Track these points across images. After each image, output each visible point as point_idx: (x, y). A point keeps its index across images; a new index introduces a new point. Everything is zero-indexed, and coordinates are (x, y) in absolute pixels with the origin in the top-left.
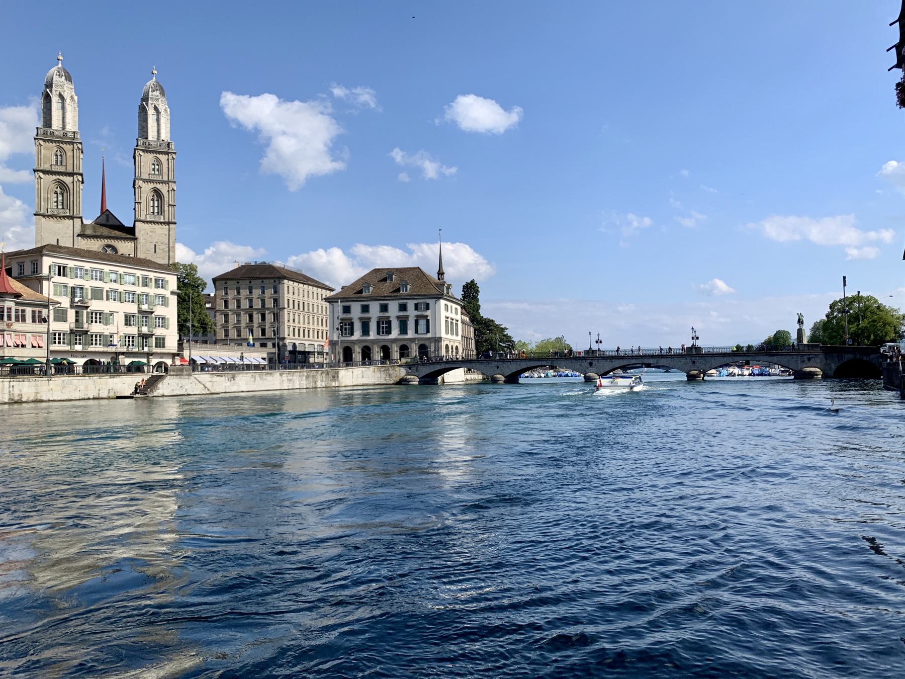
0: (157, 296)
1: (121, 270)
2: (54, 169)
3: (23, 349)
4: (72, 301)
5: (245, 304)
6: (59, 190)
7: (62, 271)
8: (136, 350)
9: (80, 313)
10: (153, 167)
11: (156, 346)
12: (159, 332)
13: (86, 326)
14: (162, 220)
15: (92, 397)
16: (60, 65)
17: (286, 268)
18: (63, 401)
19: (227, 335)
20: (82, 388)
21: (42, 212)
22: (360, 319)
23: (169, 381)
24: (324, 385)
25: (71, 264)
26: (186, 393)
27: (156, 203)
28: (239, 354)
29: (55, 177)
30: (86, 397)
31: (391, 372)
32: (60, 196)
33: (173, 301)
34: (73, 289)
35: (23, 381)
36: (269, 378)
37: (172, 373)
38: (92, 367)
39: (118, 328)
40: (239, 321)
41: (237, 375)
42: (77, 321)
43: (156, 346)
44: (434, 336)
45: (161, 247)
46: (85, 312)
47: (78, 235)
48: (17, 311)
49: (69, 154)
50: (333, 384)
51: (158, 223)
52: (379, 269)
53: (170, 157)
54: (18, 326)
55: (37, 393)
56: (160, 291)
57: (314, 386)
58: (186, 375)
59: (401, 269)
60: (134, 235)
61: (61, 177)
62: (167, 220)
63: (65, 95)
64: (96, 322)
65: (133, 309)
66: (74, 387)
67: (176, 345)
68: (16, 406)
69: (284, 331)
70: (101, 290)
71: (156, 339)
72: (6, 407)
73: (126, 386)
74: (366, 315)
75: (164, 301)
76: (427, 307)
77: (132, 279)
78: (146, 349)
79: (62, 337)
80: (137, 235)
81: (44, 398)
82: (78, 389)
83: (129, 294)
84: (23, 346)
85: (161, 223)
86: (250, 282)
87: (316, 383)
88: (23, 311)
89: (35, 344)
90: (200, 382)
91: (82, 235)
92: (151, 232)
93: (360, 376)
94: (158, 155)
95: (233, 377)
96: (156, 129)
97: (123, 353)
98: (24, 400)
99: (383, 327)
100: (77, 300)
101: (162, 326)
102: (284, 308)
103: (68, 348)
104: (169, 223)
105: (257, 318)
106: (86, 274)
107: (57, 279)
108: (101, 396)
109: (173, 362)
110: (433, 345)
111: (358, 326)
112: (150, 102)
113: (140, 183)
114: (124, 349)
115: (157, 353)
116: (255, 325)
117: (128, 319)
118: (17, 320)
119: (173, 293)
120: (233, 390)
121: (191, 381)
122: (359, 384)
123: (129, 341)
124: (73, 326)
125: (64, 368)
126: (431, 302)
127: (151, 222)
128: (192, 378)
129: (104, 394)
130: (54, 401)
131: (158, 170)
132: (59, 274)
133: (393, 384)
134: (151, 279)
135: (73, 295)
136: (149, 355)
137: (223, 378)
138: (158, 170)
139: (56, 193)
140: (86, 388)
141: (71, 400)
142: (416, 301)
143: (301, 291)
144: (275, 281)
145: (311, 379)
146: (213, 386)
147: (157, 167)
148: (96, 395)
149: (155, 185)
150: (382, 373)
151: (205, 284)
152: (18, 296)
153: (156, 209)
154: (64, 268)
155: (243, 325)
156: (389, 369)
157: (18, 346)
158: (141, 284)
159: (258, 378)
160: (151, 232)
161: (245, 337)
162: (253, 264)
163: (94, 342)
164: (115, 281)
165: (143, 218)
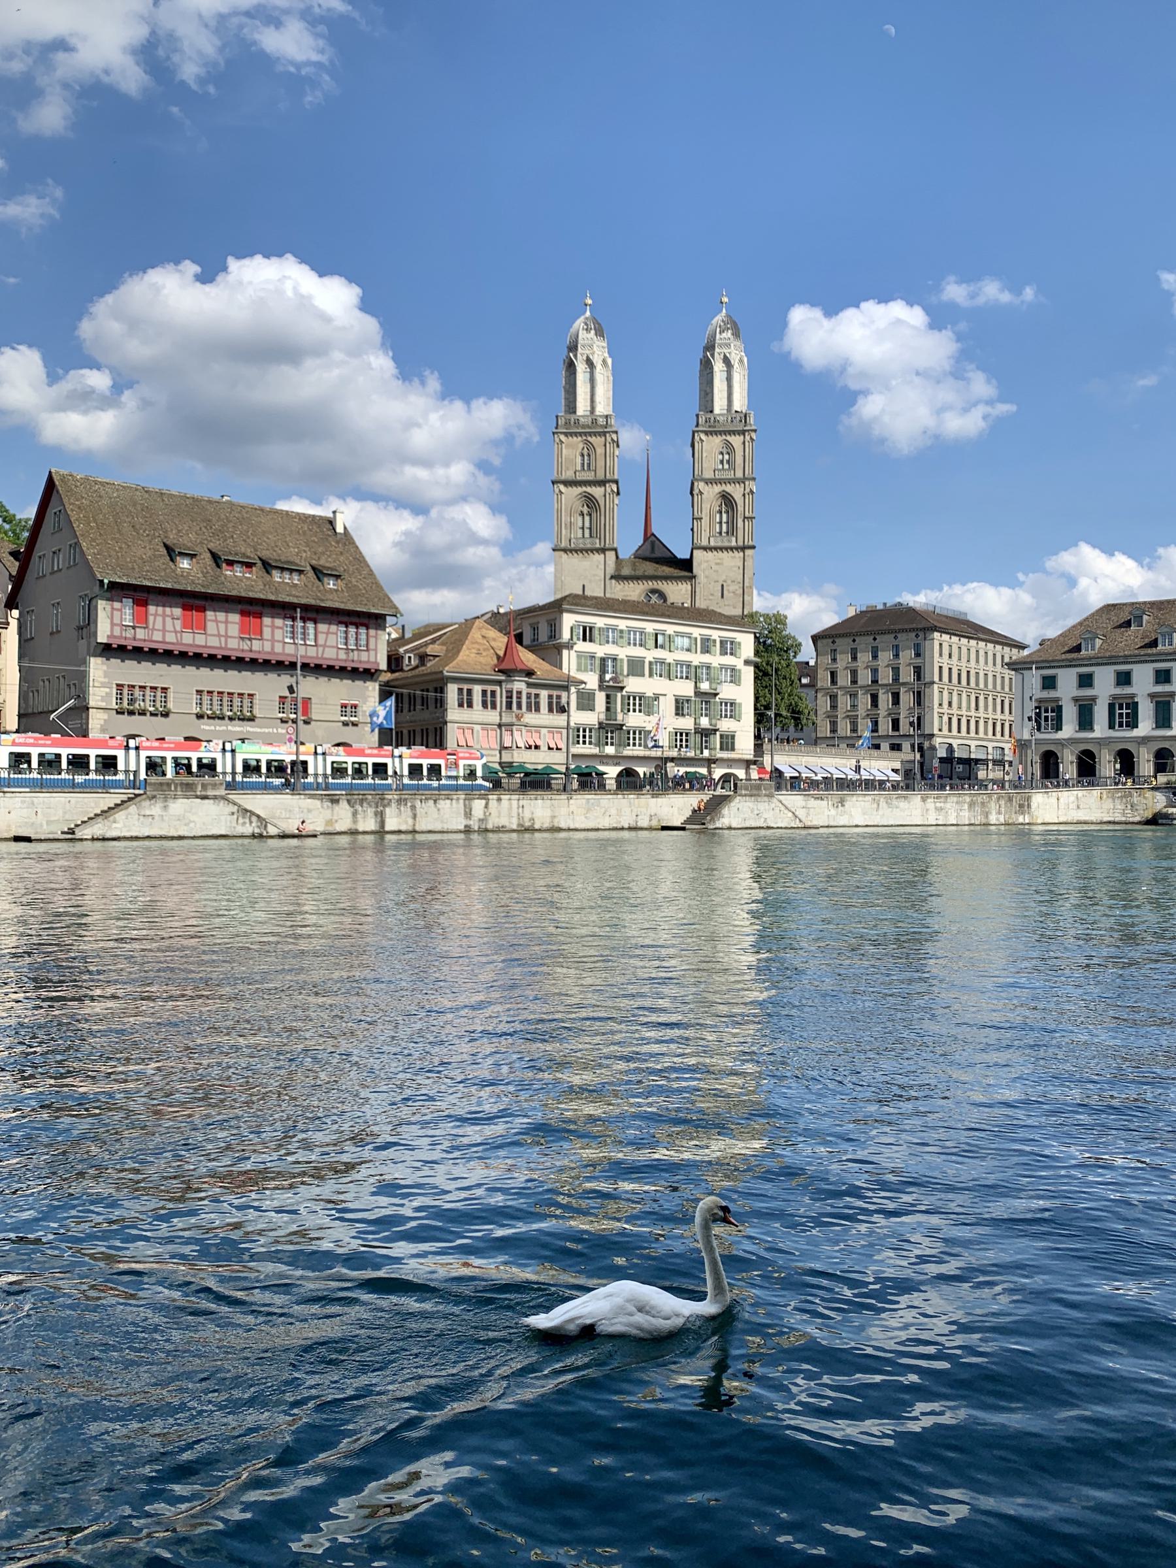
0: (723, 667)
1: (670, 629)
4: (602, 680)
5: (865, 678)
7: (588, 634)
8: (691, 754)
10: (720, 457)
11: (721, 749)
12: (725, 725)
13: (620, 716)
14: (734, 544)
15: (626, 826)
16: (588, 314)
18: (588, 830)
19: (834, 731)
20: (613, 811)
21: (563, 545)
22: (1076, 700)
23: (740, 806)
24: (1002, 820)
25: (600, 622)
26: (764, 825)
27: (724, 516)
28: (854, 762)
29: (580, 490)
30: (619, 826)
31: (1135, 800)
32: (587, 518)
33: (748, 674)
34: (603, 660)
36: (903, 804)
38: (629, 781)
40: (854, 706)
41: (848, 798)
42: (608, 709)
45: (732, 588)
46: (619, 695)
47: (612, 577)
48: (529, 696)
49: (600, 451)
50: (1021, 819)
51: (726, 549)
52: (1114, 605)
54: (530, 718)
55: (553, 817)
56: (728, 660)
57: (984, 821)
59: (1162, 602)
60: (691, 570)
61: (588, 489)
62: (740, 543)
63: (597, 361)
65: (686, 688)
67: (752, 747)
68: (527, 836)
71: (721, 736)
72: (514, 835)
73: (675, 809)
74: (1088, 692)
75: (735, 677)
77: (686, 641)
78: (706, 753)
79: (587, 734)
81: (563, 825)
83: (682, 666)
84: (537, 747)
85: (732, 549)
86: (875, 639)
87: (987, 817)
88: (537, 696)
89: (553, 745)
90: (786, 808)
91: (617, 577)
92: (717, 564)
93: (1073, 806)
94: (728, 438)
95: (842, 802)
97: (672, 760)
98: (537, 826)
99: (1121, 715)
100: (608, 677)
102: (933, 683)
103: (595, 750)
104: (743, 549)
105: (885, 699)
106: (621, 637)
107: (581, 646)
108: (640, 824)
109: (747, 773)
111: (1070, 714)
112: (717, 350)
113: (701, 485)
114: (674, 753)
115: (722, 760)
118: (529, 709)
119: (747, 662)
120: (841, 823)
122: (1070, 819)
123: (681, 740)
124: (603, 717)
125: (589, 781)
127: (716, 549)
128: (774, 800)
129: (644, 823)
130: (576, 830)
131: (728, 462)
132: (584, 639)
133: (1139, 823)
134: (715, 641)
135: (603, 671)
136: (710, 762)
137: (825, 803)
138: (728, 462)
139: (582, 514)
140: (619, 811)
141: (598, 830)
143: (964, 650)
144: (917, 636)
145: (978, 809)
147: (726, 457)
148: (633, 824)
149: (724, 487)
150: (1117, 802)
151: (800, 644)
152: (530, 673)
153: (724, 526)
155: (861, 712)
157: (530, 747)
160: (717, 564)
162: (880, 607)
163: (631, 741)
165: (704, 543)
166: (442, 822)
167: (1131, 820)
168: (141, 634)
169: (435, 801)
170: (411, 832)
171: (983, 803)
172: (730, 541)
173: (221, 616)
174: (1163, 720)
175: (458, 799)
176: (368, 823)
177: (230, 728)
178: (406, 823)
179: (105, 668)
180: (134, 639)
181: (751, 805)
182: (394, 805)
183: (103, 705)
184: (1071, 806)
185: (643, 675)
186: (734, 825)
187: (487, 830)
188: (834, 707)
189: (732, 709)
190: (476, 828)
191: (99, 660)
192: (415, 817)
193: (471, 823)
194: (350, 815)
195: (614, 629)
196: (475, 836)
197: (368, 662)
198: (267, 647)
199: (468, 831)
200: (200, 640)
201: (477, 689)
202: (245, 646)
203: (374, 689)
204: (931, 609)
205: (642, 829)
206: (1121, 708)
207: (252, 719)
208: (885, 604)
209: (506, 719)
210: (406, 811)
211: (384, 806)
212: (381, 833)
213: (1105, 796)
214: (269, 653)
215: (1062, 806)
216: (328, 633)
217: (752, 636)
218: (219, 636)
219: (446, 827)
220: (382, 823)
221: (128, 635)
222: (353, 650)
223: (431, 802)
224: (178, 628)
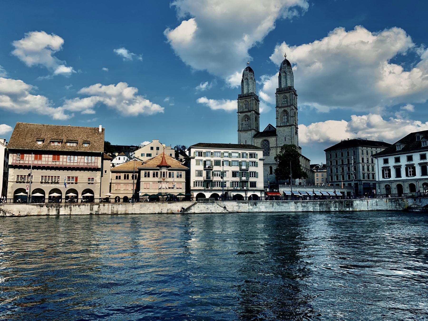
1: (230, 151)
3: (172, 190)
5: (340, 162)
6: (246, 119)
7: (200, 154)
8: (239, 188)
9: (209, 172)
11: (251, 187)
12: (252, 179)
13: (211, 178)
14: (288, 125)
15: (157, 212)
22: (395, 167)
23: (199, 206)
24: (337, 209)
25: (204, 150)
28: (312, 190)
29: (244, 114)
30: (154, 213)
33: (261, 164)
34: (205, 162)
35: (119, 205)
36: (285, 205)
37: (200, 201)
38: (215, 197)
39: (229, 178)
41: (258, 203)
43: (251, 187)
45: (288, 138)
46: (211, 171)
47: (253, 137)
50: (348, 209)
51: (286, 126)
53: (291, 93)
55: (126, 210)
57: (327, 210)
61: (247, 114)
62: (290, 124)
65: (237, 169)
66: (147, 208)
68: (115, 216)
69: (360, 176)
70: (219, 161)
71: (251, 183)
77: (237, 155)
78: (245, 188)
79: (200, 183)
82: (149, 209)
85: (287, 126)
87: (329, 209)
90: (220, 206)
91: (255, 136)
93: (375, 204)
95: (255, 204)
96: (285, 82)
98: (119, 213)
99: (410, 171)
100: (207, 166)
101: (255, 177)
105: (346, 168)
106: (212, 155)
107: (197, 158)
108: (163, 212)
111: (393, 172)
114: (232, 188)
116: (345, 173)
117: (234, 174)
119: (260, 160)
121: (214, 206)
124: (205, 178)
127: (283, 126)
128: (215, 204)
129: (165, 211)
131: (286, 101)
132: (199, 156)
133: (402, 211)
134: (247, 154)
136: (246, 191)
137: (247, 204)
138: (286, 101)
139: (245, 121)
144: (354, 148)
146: (239, 208)
148: (160, 212)
154: (201, 153)
155: (339, 173)
156: (399, 201)
158: (241, 157)
159: (275, 204)
161: (340, 180)
164: (227, 157)
166: (82, 212)
168: (21, 162)
169: (79, 206)
170: (69, 215)
172: (287, 124)
173: (47, 156)
174: (424, 173)
175: (88, 205)
176: (53, 212)
177: (51, 186)
178: (68, 212)
179: (13, 171)
180: (20, 163)
181: (204, 205)
182: (63, 207)
183: (12, 181)
184: (374, 205)
186: (196, 212)
187: (98, 214)
188: (331, 172)
189: (255, 174)
190: (94, 214)
191: (12, 169)
192: (71, 210)
193: (93, 212)
194: (47, 210)
195: (209, 152)
196: (94, 216)
197: (95, 166)
198: (61, 163)
199: (91, 214)
200: (40, 162)
201: (151, 172)
202: (54, 163)
203: (99, 174)
205: (164, 213)
206: (410, 169)
207: (58, 183)
208: (348, 139)
209: (161, 180)
210: (68, 209)
211: (60, 208)
212: (58, 215)
214: (61, 165)
215: (369, 205)
216: (81, 159)
217: (262, 152)
218: (46, 161)
219: (82, 214)
220: (59, 212)
221: (18, 162)
222: (89, 163)
223: (77, 206)
224: (33, 160)
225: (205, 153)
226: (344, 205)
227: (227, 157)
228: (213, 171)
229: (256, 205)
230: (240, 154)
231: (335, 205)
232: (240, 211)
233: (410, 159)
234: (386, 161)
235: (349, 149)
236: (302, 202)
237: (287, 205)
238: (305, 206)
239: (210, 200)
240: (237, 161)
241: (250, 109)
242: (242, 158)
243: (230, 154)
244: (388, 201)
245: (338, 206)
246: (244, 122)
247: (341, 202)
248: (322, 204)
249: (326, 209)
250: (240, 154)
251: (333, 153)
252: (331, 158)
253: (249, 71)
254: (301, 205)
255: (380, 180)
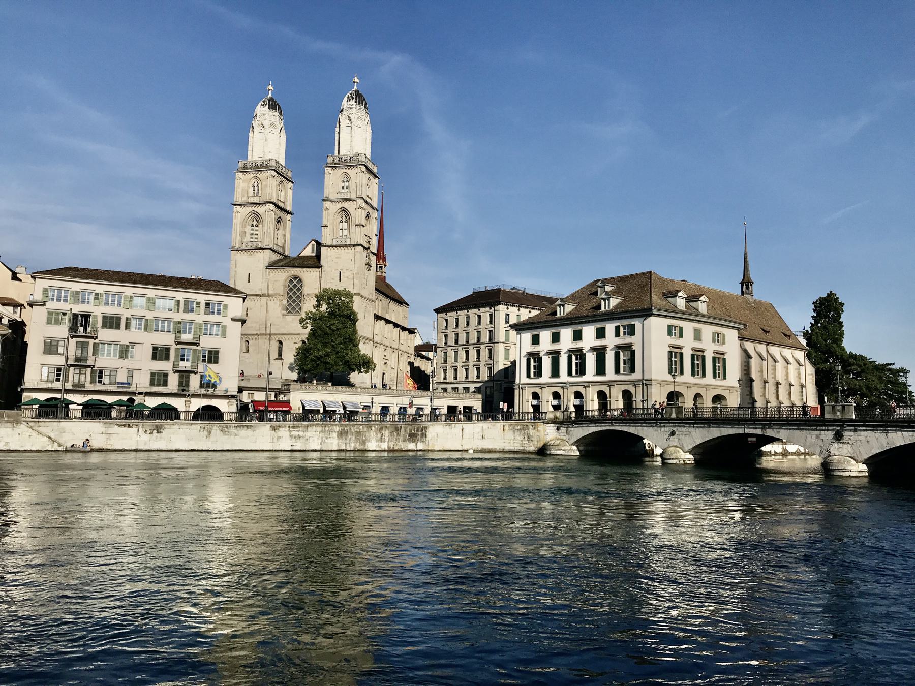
2: (251, 200)
14: (348, 243)
17: (528, 291)
24: (385, 446)
29: (251, 209)
36: (243, 432)
44: (641, 378)
46: (91, 341)
50: (411, 446)
51: (343, 246)
53: (359, 170)
57: (358, 447)
58: (8, 422)
61: (256, 209)
64: (109, 355)
65: (166, 339)
76: (631, 331)
80: (322, 262)
83: (163, 321)
85: (346, 246)
87: (364, 442)
91: (272, 266)
92: (337, 258)
94: (347, 171)
105: (473, 353)
110: (640, 389)
117: (160, 353)
121: (20, 431)
126: (637, 323)
127: (336, 246)
134: (198, 303)
137: (134, 429)
139: (252, 226)
142: (617, 324)
150: (517, 433)
160: (337, 258)
167: (527, 449)
171: (358, 433)
184: (476, 436)
185: (118, 327)
204: (523, 289)
213: (507, 428)
225: (77, 293)
226: (405, 436)
227: (141, 307)
228: (97, 341)
229: (158, 432)
230: (179, 301)
231: (379, 435)
232: (109, 447)
233: (578, 336)
234: (535, 340)
235: (482, 310)
236: (293, 427)
237: (249, 432)
238: (299, 437)
239: (8, 417)
240: (170, 320)
241: (264, 199)
242: (184, 312)
243: (151, 302)
244: (507, 428)
245: (387, 438)
246: (248, 229)
247: (397, 430)
248: (346, 433)
249: (355, 445)
250: (179, 301)
251: (451, 315)
252: (446, 327)
253: (269, 108)
254: (288, 433)
255: (522, 382)
